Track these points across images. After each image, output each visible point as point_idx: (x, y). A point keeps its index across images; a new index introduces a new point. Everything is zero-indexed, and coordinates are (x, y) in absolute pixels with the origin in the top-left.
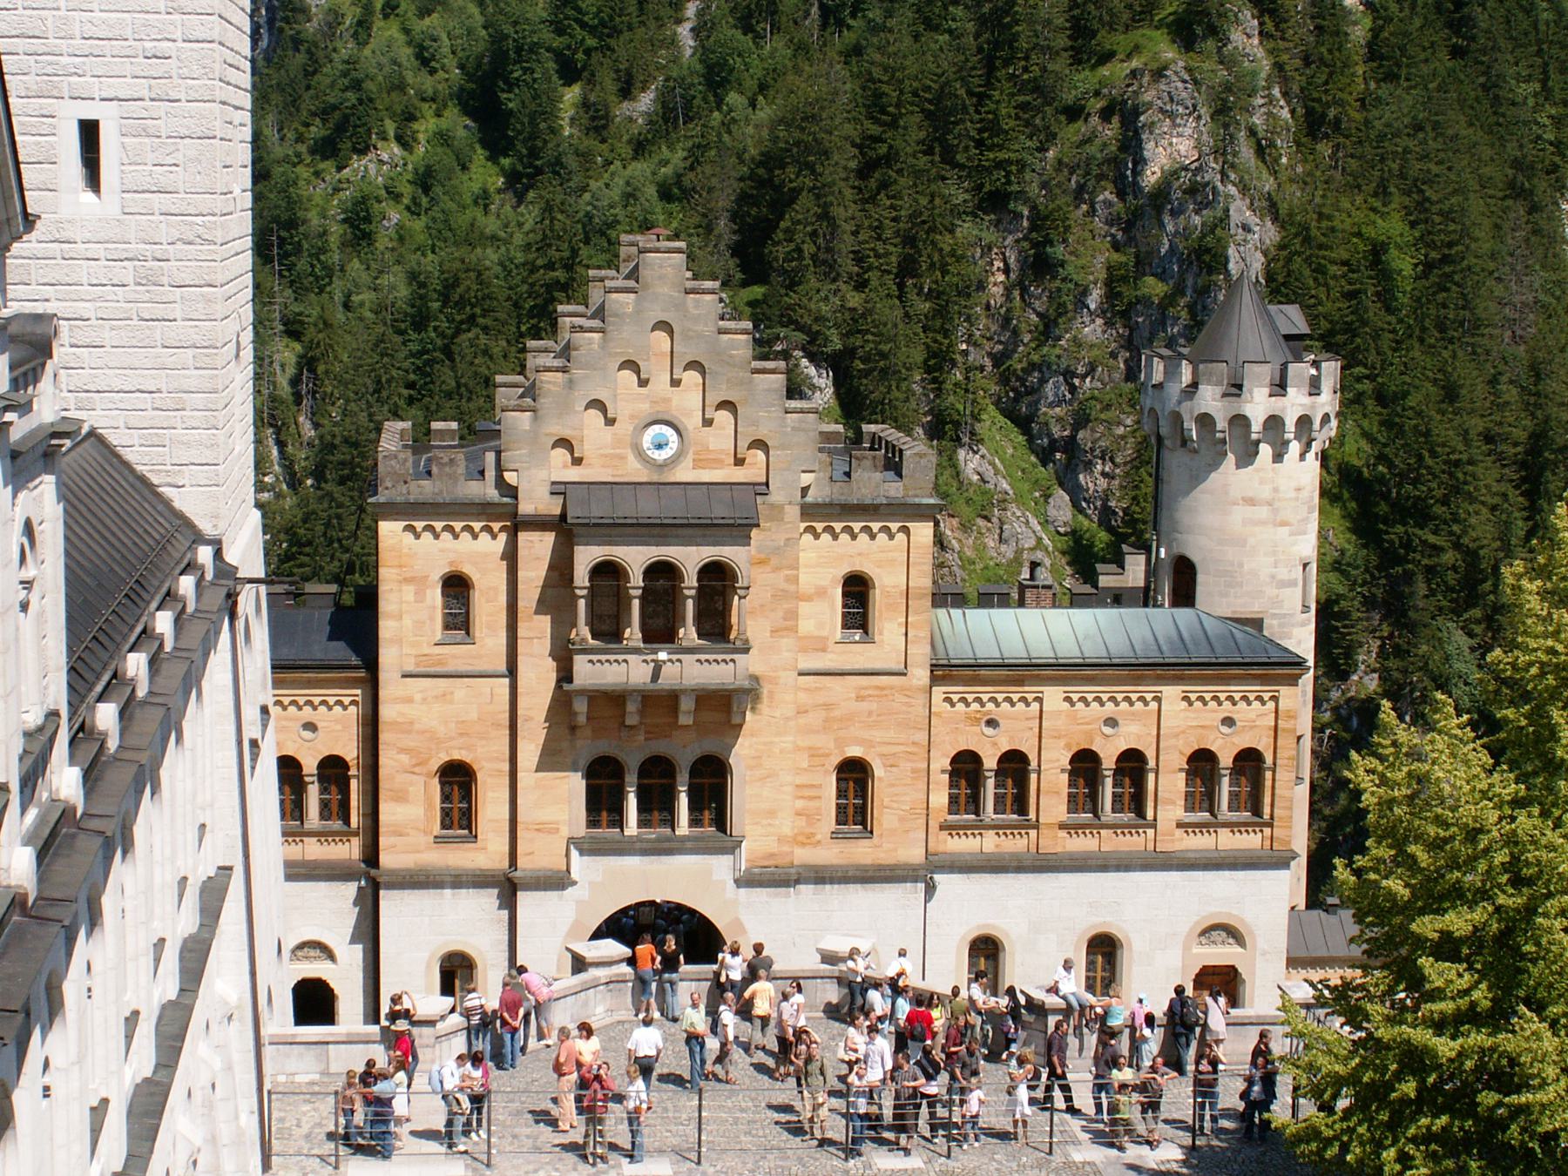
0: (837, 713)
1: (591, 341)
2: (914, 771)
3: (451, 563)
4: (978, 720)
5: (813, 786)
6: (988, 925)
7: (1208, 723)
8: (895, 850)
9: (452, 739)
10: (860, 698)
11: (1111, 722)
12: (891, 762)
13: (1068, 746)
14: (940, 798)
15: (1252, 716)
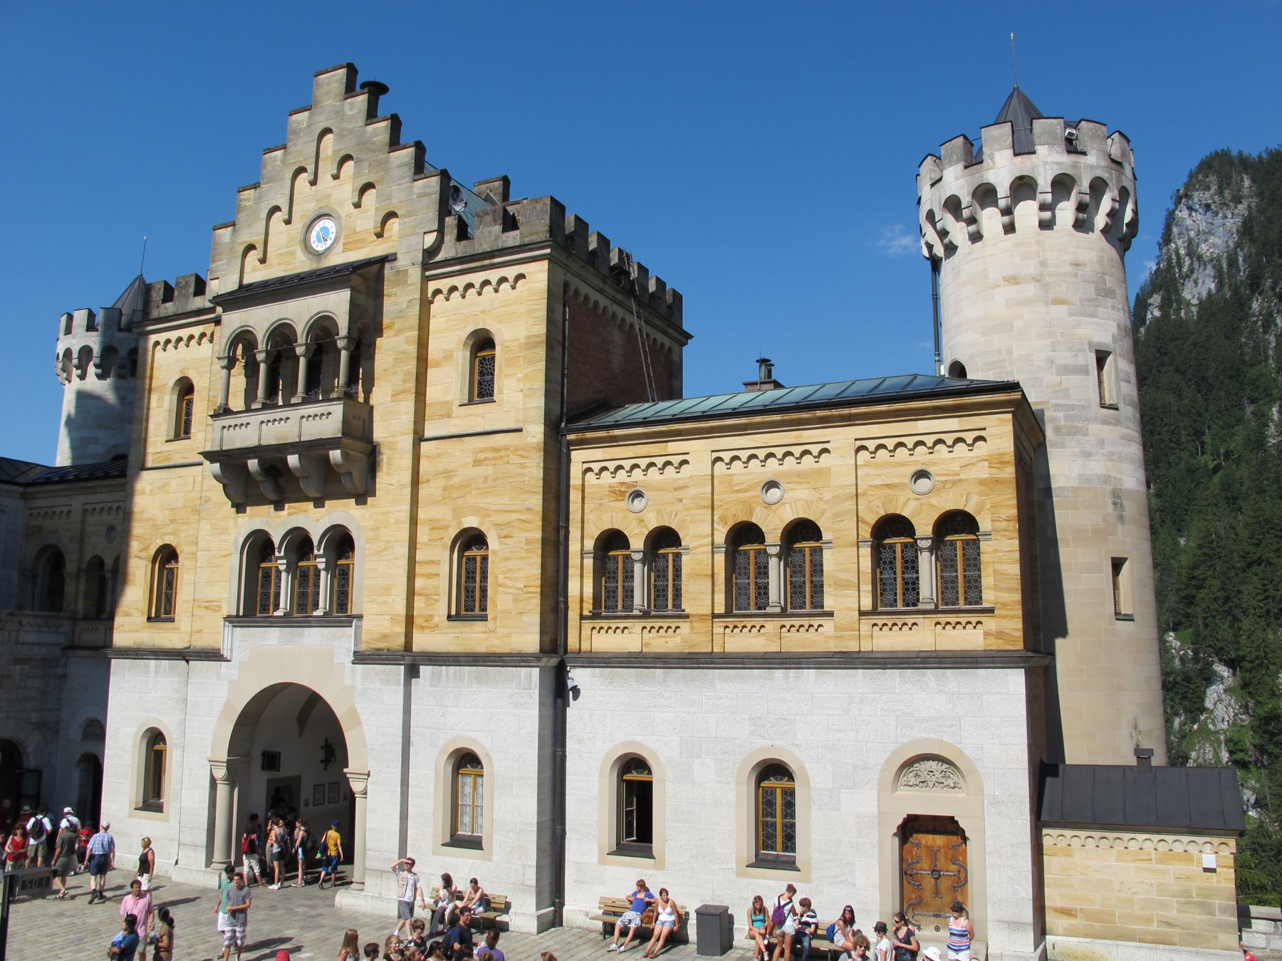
0: (456, 481)
1: (275, 159)
2: (528, 542)
3: (181, 371)
4: (622, 493)
5: (432, 562)
6: (631, 743)
7: (896, 481)
8: (509, 636)
9: (166, 525)
10: (477, 463)
11: (771, 484)
12: (506, 532)
13: (724, 520)
14: (581, 586)
15: (955, 467)
